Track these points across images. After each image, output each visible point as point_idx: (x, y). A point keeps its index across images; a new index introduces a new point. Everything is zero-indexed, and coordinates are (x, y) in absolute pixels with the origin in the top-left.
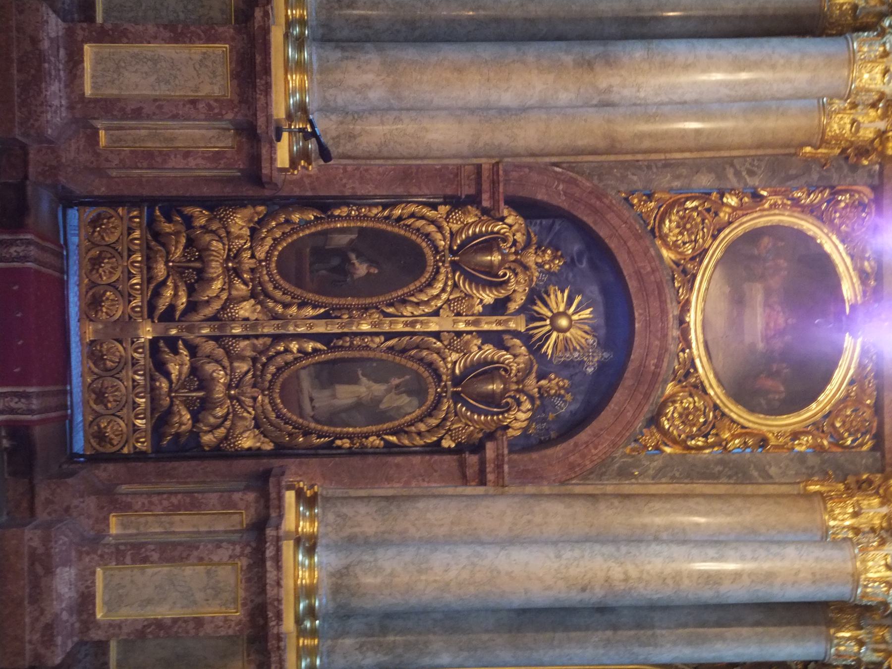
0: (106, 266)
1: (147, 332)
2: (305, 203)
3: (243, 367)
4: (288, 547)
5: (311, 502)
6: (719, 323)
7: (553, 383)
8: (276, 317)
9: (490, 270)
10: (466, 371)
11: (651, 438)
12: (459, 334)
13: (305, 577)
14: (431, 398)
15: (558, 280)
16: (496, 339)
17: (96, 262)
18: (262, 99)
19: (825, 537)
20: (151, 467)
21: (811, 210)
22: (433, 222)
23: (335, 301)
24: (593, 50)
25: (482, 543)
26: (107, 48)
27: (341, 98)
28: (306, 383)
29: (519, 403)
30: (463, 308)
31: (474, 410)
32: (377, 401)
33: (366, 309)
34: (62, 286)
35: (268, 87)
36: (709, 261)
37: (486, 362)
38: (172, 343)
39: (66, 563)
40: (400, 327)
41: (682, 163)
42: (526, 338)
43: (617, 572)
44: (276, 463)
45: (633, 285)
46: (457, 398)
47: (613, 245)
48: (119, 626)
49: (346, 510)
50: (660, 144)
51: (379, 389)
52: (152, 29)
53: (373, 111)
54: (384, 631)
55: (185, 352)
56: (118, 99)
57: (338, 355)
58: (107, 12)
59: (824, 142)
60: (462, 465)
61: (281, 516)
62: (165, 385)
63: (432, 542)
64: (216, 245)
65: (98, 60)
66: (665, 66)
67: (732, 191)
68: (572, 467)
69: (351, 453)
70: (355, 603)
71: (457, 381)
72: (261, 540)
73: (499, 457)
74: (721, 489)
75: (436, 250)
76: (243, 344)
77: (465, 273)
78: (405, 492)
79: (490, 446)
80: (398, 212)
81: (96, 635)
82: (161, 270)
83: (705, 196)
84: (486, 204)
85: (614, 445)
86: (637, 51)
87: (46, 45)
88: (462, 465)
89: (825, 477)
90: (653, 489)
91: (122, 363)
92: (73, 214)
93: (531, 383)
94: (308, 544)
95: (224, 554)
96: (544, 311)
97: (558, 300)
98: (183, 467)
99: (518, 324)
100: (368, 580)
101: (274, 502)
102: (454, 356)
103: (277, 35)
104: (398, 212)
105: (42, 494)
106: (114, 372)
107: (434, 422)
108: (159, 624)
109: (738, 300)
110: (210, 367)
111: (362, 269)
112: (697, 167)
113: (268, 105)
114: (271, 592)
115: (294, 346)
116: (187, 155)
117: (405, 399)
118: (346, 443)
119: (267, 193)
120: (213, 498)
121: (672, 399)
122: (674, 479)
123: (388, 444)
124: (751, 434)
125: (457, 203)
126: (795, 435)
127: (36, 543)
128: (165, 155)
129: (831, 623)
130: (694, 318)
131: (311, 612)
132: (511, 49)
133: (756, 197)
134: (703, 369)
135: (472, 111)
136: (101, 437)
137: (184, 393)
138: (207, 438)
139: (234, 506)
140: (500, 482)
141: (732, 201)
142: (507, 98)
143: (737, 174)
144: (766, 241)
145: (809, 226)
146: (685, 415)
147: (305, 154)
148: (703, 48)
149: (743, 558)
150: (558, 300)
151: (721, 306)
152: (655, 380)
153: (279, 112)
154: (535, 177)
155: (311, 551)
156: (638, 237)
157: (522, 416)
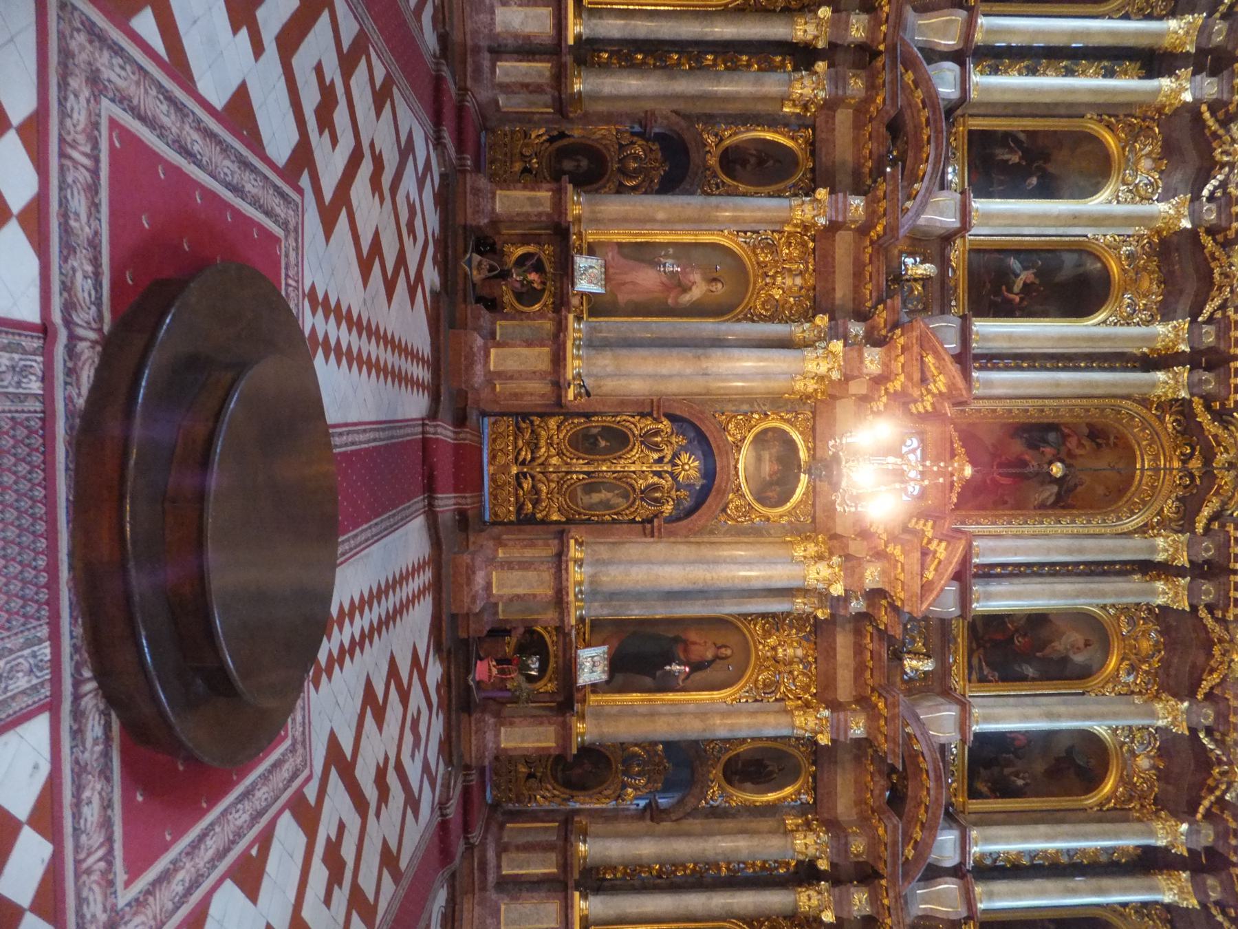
0: (498, 441)
3: (553, 485)
4: (571, 564)
5: (581, 544)
6: (751, 469)
7: (683, 493)
8: (567, 464)
10: (646, 488)
11: (722, 518)
12: (643, 472)
13: (578, 577)
14: (631, 499)
15: (685, 449)
16: (658, 474)
17: (494, 440)
18: (562, 371)
19: (792, 560)
20: (516, 528)
21: (788, 421)
22: (633, 423)
23: (592, 457)
24: (700, 351)
25: (652, 563)
26: (500, 350)
27: (595, 370)
28: (579, 493)
29: (668, 502)
30: (645, 461)
31: (649, 505)
32: (608, 500)
33: (604, 460)
34: (481, 450)
35: (565, 365)
36: (747, 442)
37: (654, 484)
39: (481, 569)
40: (619, 469)
41: (736, 400)
42: (671, 474)
43: (708, 576)
44: (566, 527)
45: (716, 452)
46: (642, 499)
47: (708, 435)
48: (501, 596)
49: (596, 548)
50: (727, 392)
51: (610, 495)
52: (518, 342)
53: (609, 376)
54: (611, 600)
55: (530, 479)
56: (503, 372)
57: (593, 480)
58: (501, 335)
59: (793, 393)
60: (644, 529)
61: (568, 551)
62: (521, 493)
63: (631, 563)
64: (543, 433)
65: (497, 355)
66: (730, 359)
67: (756, 412)
68: (690, 530)
69: (598, 522)
70: (599, 589)
71: (642, 492)
72: (560, 562)
73: (660, 525)
74: (751, 540)
75: (634, 435)
76: (554, 475)
77: (645, 445)
78: (621, 540)
79: (656, 522)
80: (618, 419)
81: (493, 600)
82: (520, 443)
83: (745, 414)
84: (655, 416)
85: (707, 521)
86: (718, 352)
87: (475, 349)
88: (644, 529)
89: (792, 534)
90: (724, 540)
91: (505, 484)
92: (486, 419)
93: (673, 493)
94: (580, 563)
95: (544, 567)
96: (679, 462)
97: (685, 457)
98: (528, 528)
99: (668, 468)
100: (604, 579)
101: (565, 545)
102: (641, 481)
103: (569, 344)
104: (618, 419)
105: (472, 539)
106: (501, 487)
107: (632, 510)
108: (518, 596)
109: (759, 459)
110: (540, 485)
111: (603, 443)
112: (742, 402)
113: (565, 373)
114: (564, 584)
115: (575, 476)
116: (532, 394)
117: (620, 500)
118: (596, 518)
119: (564, 411)
120: (540, 542)
121: (731, 501)
122: (732, 535)
123: (613, 519)
124: (763, 516)
126: (781, 516)
127: (469, 561)
128: (523, 395)
129: (794, 596)
130: (741, 466)
131: (581, 592)
132: (666, 350)
133: (766, 415)
134: (744, 488)
135: (650, 376)
136: (496, 515)
137: (529, 496)
138: (539, 516)
139: (549, 546)
140: (660, 536)
141: (756, 416)
142: (664, 370)
143: (758, 405)
144: (770, 434)
145: (787, 427)
146: (737, 507)
147: (580, 394)
148: (745, 352)
149: (760, 570)
150: (685, 457)
151: (752, 461)
152: (724, 493)
153: (569, 376)
154: (675, 404)
155: (580, 566)
156: (719, 432)
157: (669, 507)
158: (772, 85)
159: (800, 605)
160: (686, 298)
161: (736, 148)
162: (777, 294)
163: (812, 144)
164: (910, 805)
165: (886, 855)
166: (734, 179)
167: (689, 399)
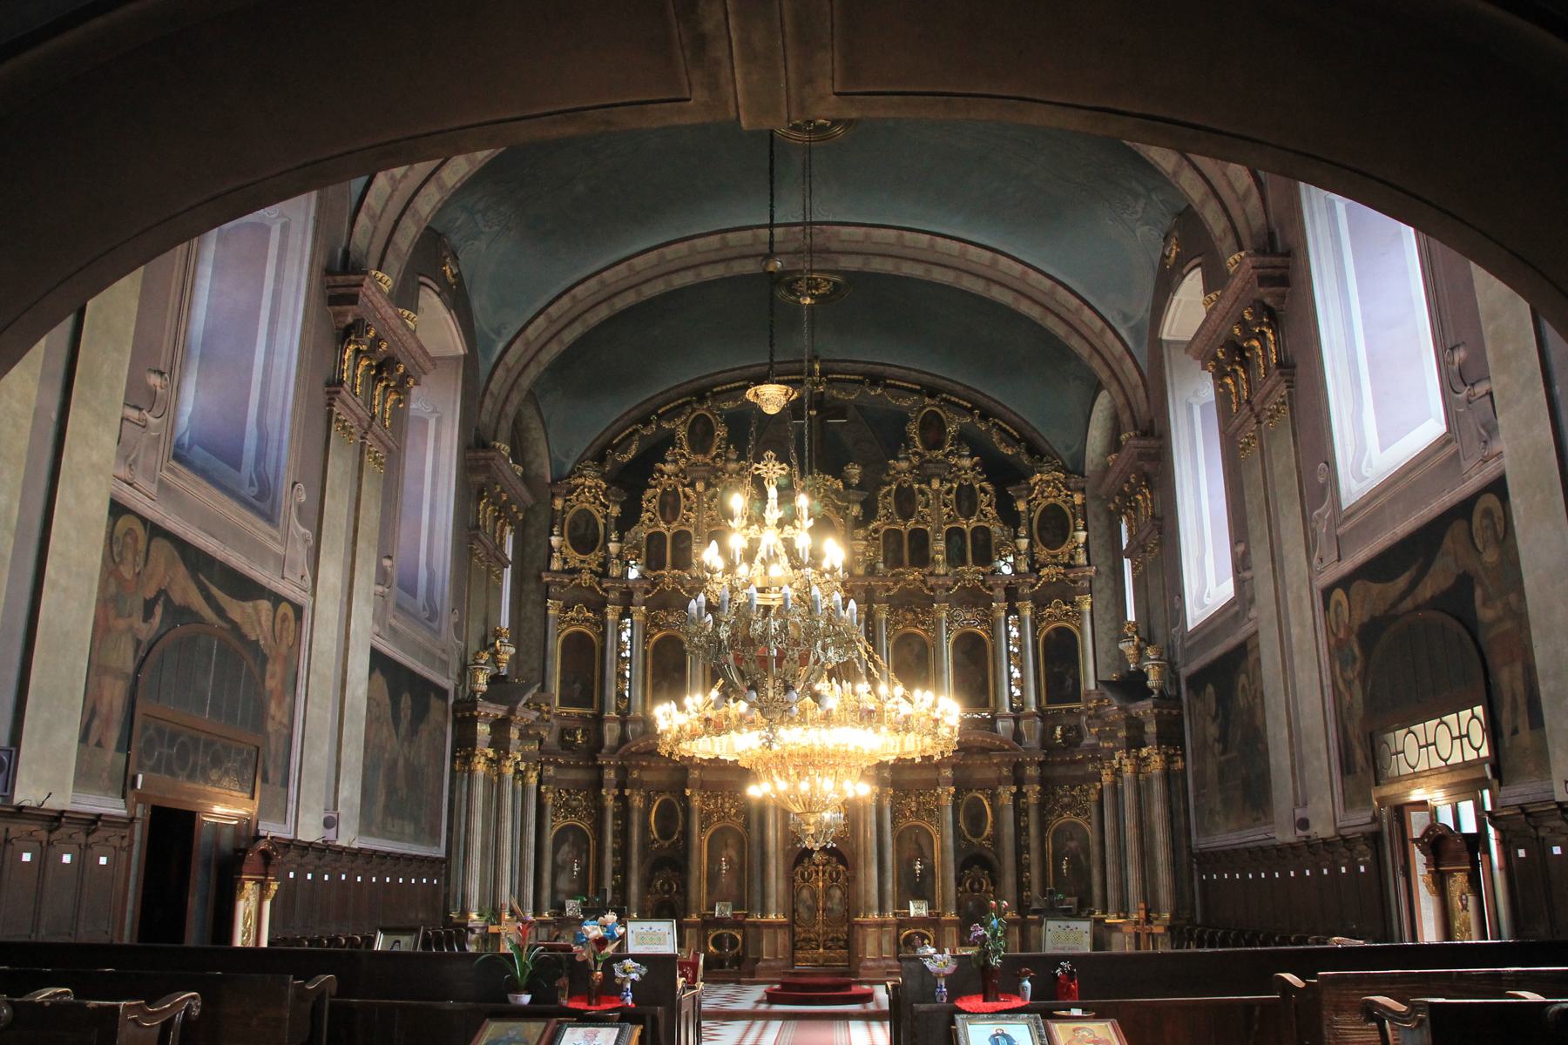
1: (821, 950)
2: (794, 916)
9: (809, 874)
38: (824, 945)
125: (794, 881)
158: (635, 818)
159: (887, 803)
160: (735, 859)
161: (659, 831)
162: (733, 811)
163: (658, 792)
164: (984, 745)
165: (1007, 760)
166: (674, 834)
167: (786, 855)
